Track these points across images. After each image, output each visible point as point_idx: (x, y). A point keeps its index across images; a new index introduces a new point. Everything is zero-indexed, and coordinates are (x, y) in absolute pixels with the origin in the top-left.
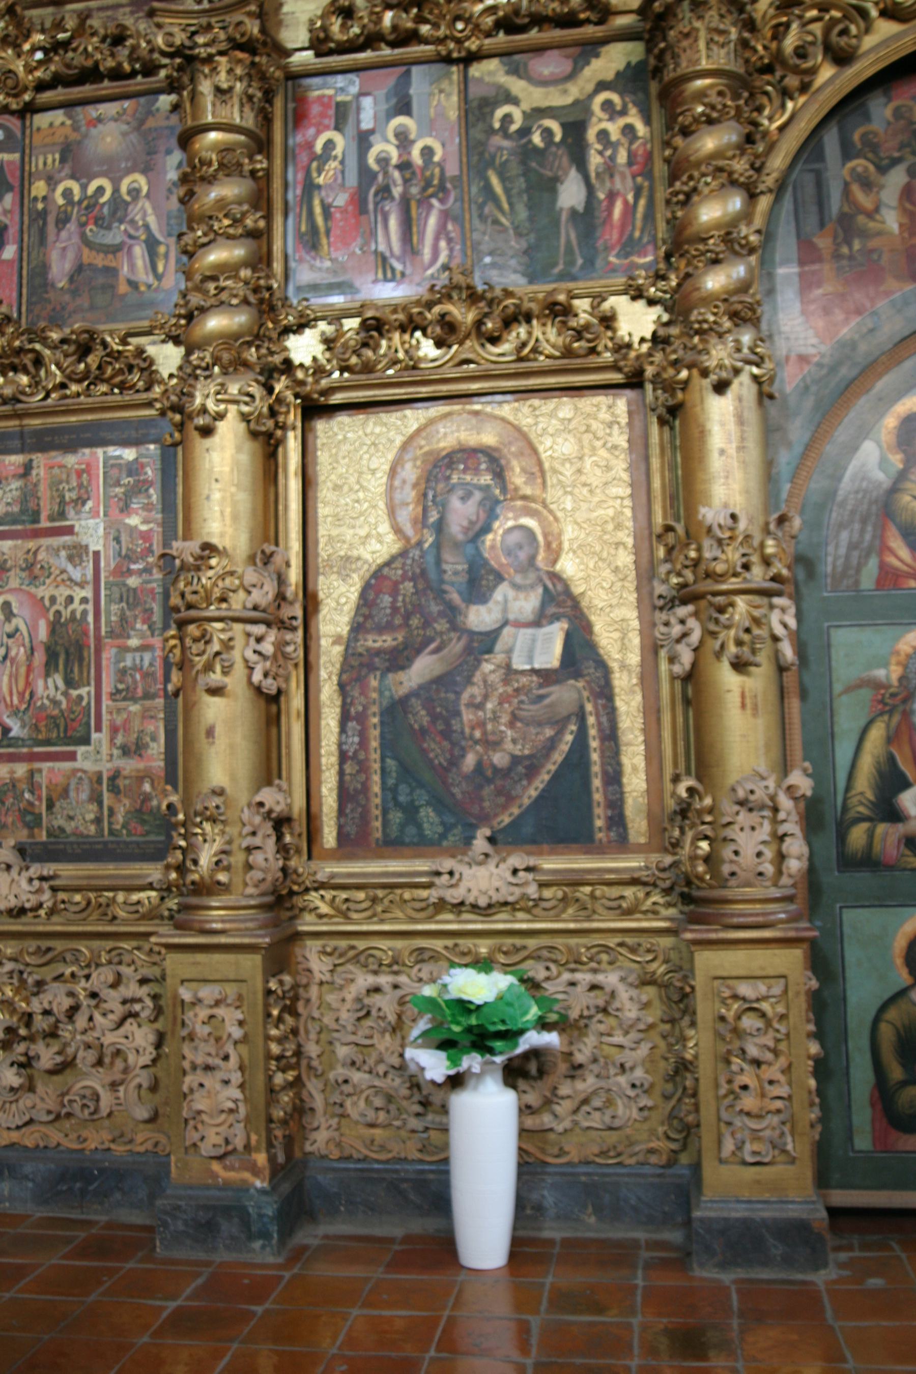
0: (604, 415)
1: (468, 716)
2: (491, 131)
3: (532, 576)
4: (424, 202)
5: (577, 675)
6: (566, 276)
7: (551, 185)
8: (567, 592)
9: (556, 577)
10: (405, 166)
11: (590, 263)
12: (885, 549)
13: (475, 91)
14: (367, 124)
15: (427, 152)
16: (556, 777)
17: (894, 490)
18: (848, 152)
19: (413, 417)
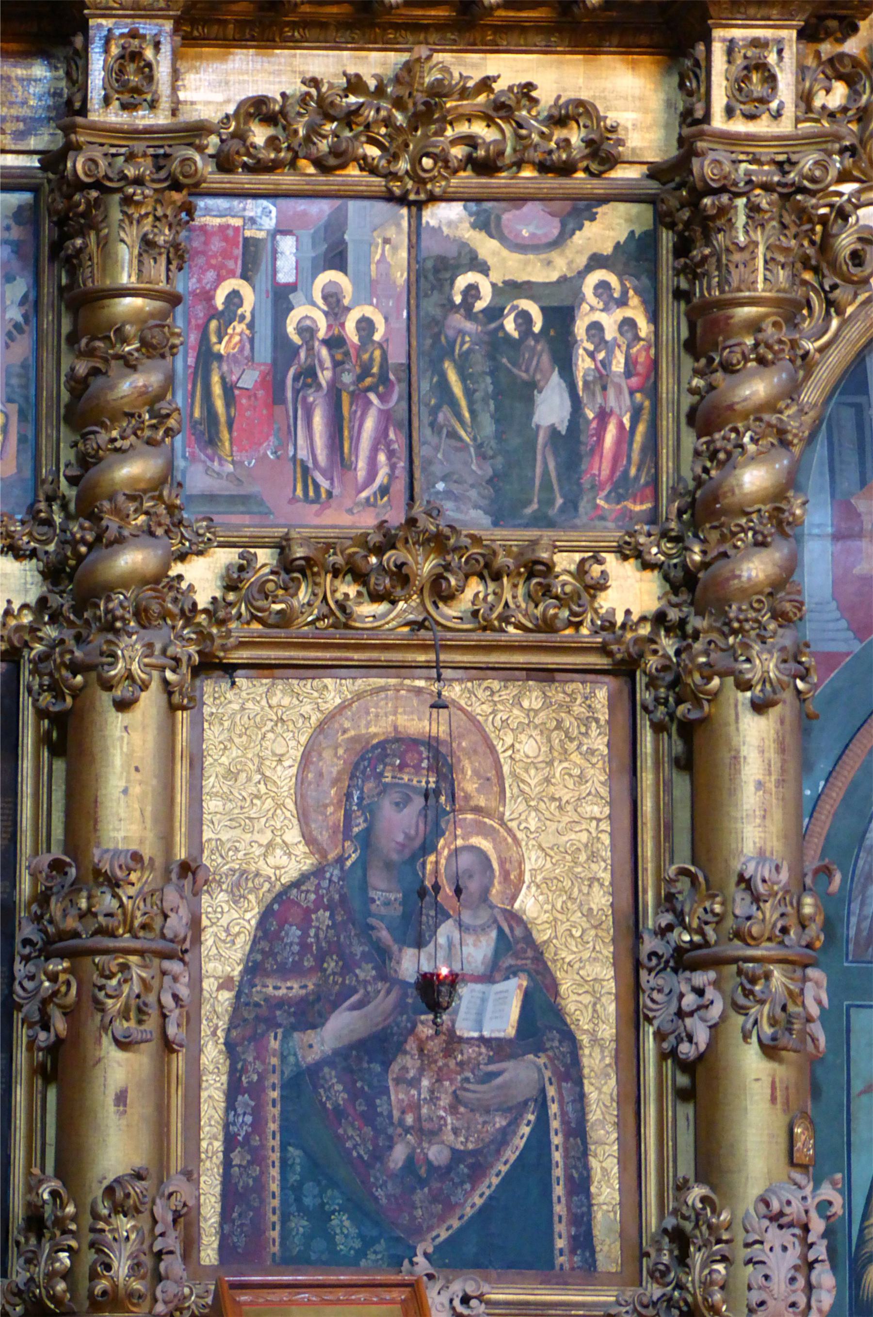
0: (578, 709)
1: (398, 1095)
2: (450, 306)
3: (484, 916)
4: (359, 396)
5: (539, 1049)
6: (542, 521)
8: (528, 937)
9: (515, 918)
10: (335, 342)
11: (571, 504)
13: (430, 246)
14: (286, 273)
15: (366, 326)
16: (507, 1180)
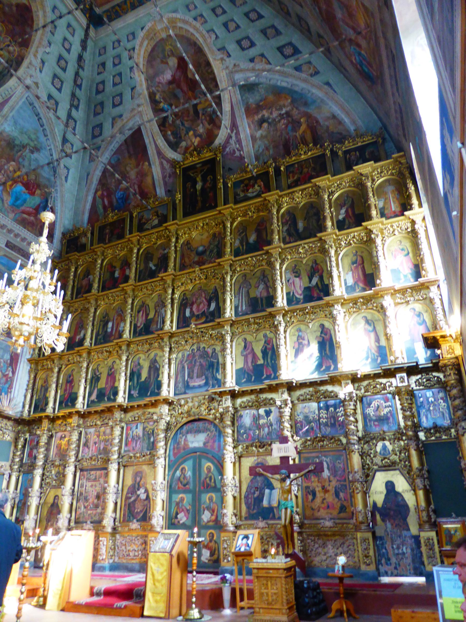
7: (149, 438)
12: (178, 484)
17: (180, 477)
18: (180, 434)
19: (135, 467)
